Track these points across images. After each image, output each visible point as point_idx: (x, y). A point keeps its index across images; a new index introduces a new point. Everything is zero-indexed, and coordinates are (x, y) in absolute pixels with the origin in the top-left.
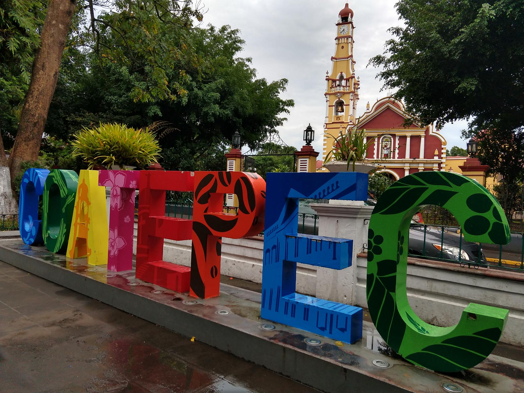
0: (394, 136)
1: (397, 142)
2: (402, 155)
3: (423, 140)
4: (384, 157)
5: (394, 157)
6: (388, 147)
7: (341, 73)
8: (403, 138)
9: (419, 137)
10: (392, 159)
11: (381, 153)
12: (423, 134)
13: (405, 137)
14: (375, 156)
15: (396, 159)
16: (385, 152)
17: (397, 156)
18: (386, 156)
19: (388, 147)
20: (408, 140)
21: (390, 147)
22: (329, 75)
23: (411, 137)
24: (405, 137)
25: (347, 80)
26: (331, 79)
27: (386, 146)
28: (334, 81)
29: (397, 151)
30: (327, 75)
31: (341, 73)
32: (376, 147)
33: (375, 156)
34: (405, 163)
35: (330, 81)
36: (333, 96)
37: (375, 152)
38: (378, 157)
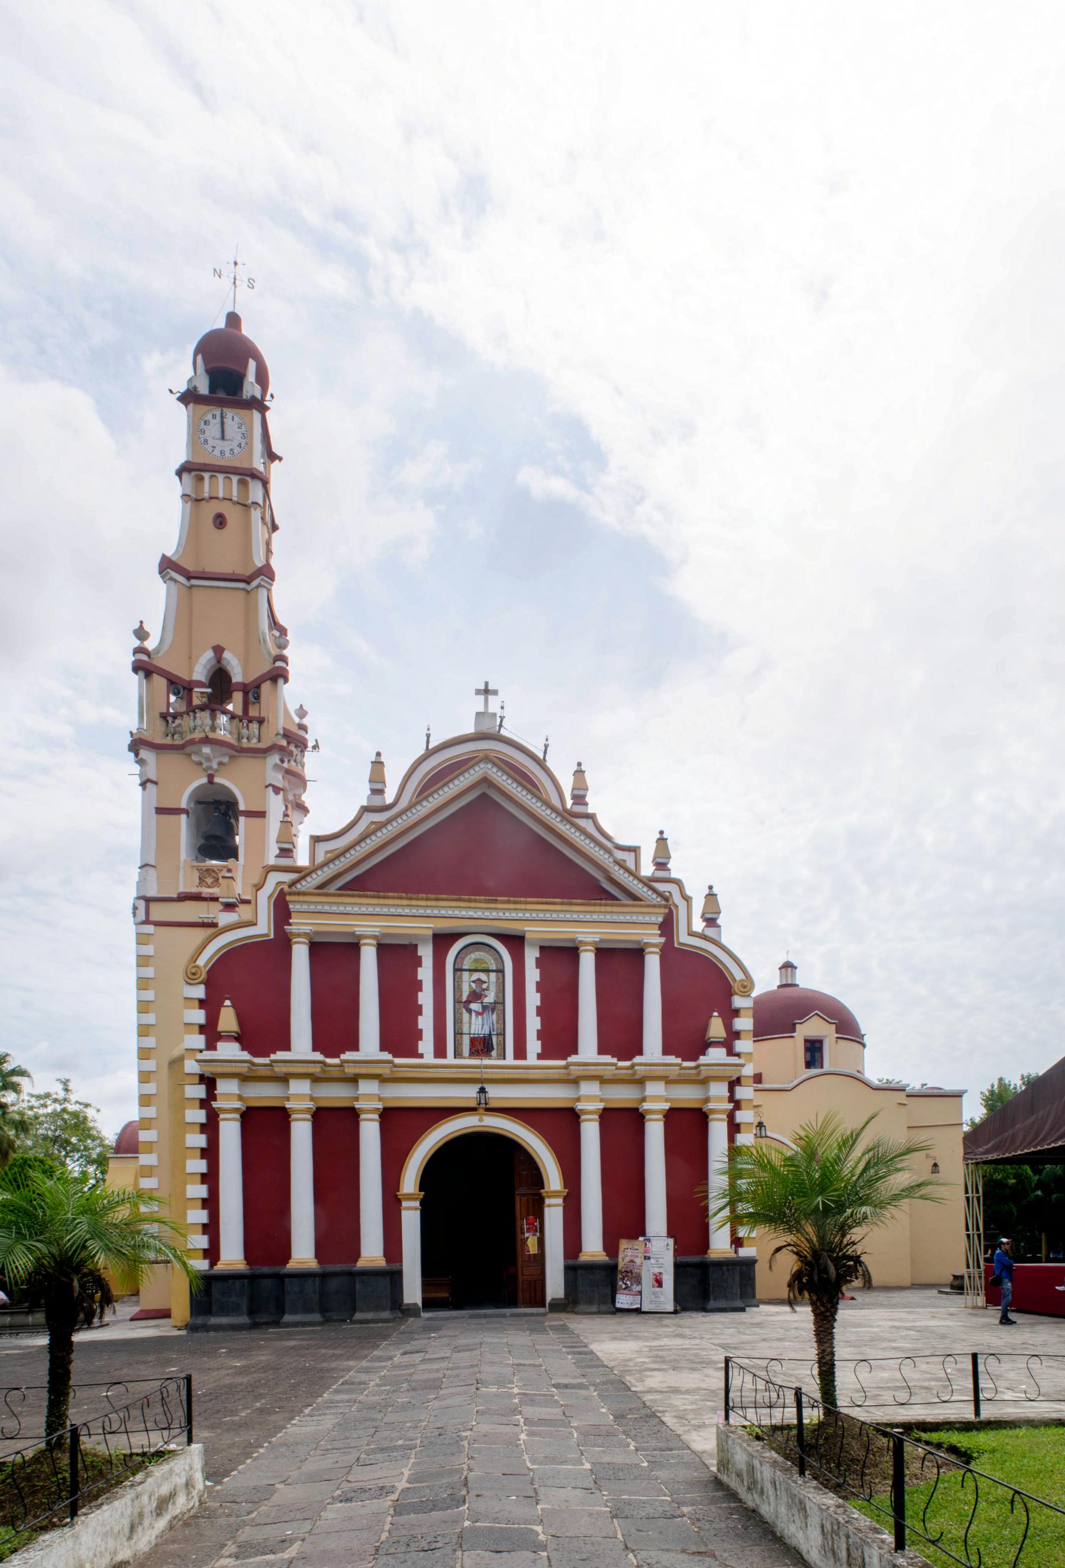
0: (515, 942)
1: (532, 975)
3: (653, 965)
5: (520, 1052)
6: (490, 998)
8: (561, 958)
9: (636, 955)
11: (458, 1034)
12: (653, 938)
13: (570, 953)
15: (532, 1059)
16: (477, 1025)
17: (534, 1046)
18: (482, 1046)
19: (490, 998)
20: (587, 962)
21: (498, 1006)
22: (151, 644)
23: (604, 954)
24: (570, 953)
27: (475, 996)
30: (137, 643)
32: (426, 998)
33: (426, 1045)
34: (575, 1082)
37: (426, 1022)
38: (440, 1051)
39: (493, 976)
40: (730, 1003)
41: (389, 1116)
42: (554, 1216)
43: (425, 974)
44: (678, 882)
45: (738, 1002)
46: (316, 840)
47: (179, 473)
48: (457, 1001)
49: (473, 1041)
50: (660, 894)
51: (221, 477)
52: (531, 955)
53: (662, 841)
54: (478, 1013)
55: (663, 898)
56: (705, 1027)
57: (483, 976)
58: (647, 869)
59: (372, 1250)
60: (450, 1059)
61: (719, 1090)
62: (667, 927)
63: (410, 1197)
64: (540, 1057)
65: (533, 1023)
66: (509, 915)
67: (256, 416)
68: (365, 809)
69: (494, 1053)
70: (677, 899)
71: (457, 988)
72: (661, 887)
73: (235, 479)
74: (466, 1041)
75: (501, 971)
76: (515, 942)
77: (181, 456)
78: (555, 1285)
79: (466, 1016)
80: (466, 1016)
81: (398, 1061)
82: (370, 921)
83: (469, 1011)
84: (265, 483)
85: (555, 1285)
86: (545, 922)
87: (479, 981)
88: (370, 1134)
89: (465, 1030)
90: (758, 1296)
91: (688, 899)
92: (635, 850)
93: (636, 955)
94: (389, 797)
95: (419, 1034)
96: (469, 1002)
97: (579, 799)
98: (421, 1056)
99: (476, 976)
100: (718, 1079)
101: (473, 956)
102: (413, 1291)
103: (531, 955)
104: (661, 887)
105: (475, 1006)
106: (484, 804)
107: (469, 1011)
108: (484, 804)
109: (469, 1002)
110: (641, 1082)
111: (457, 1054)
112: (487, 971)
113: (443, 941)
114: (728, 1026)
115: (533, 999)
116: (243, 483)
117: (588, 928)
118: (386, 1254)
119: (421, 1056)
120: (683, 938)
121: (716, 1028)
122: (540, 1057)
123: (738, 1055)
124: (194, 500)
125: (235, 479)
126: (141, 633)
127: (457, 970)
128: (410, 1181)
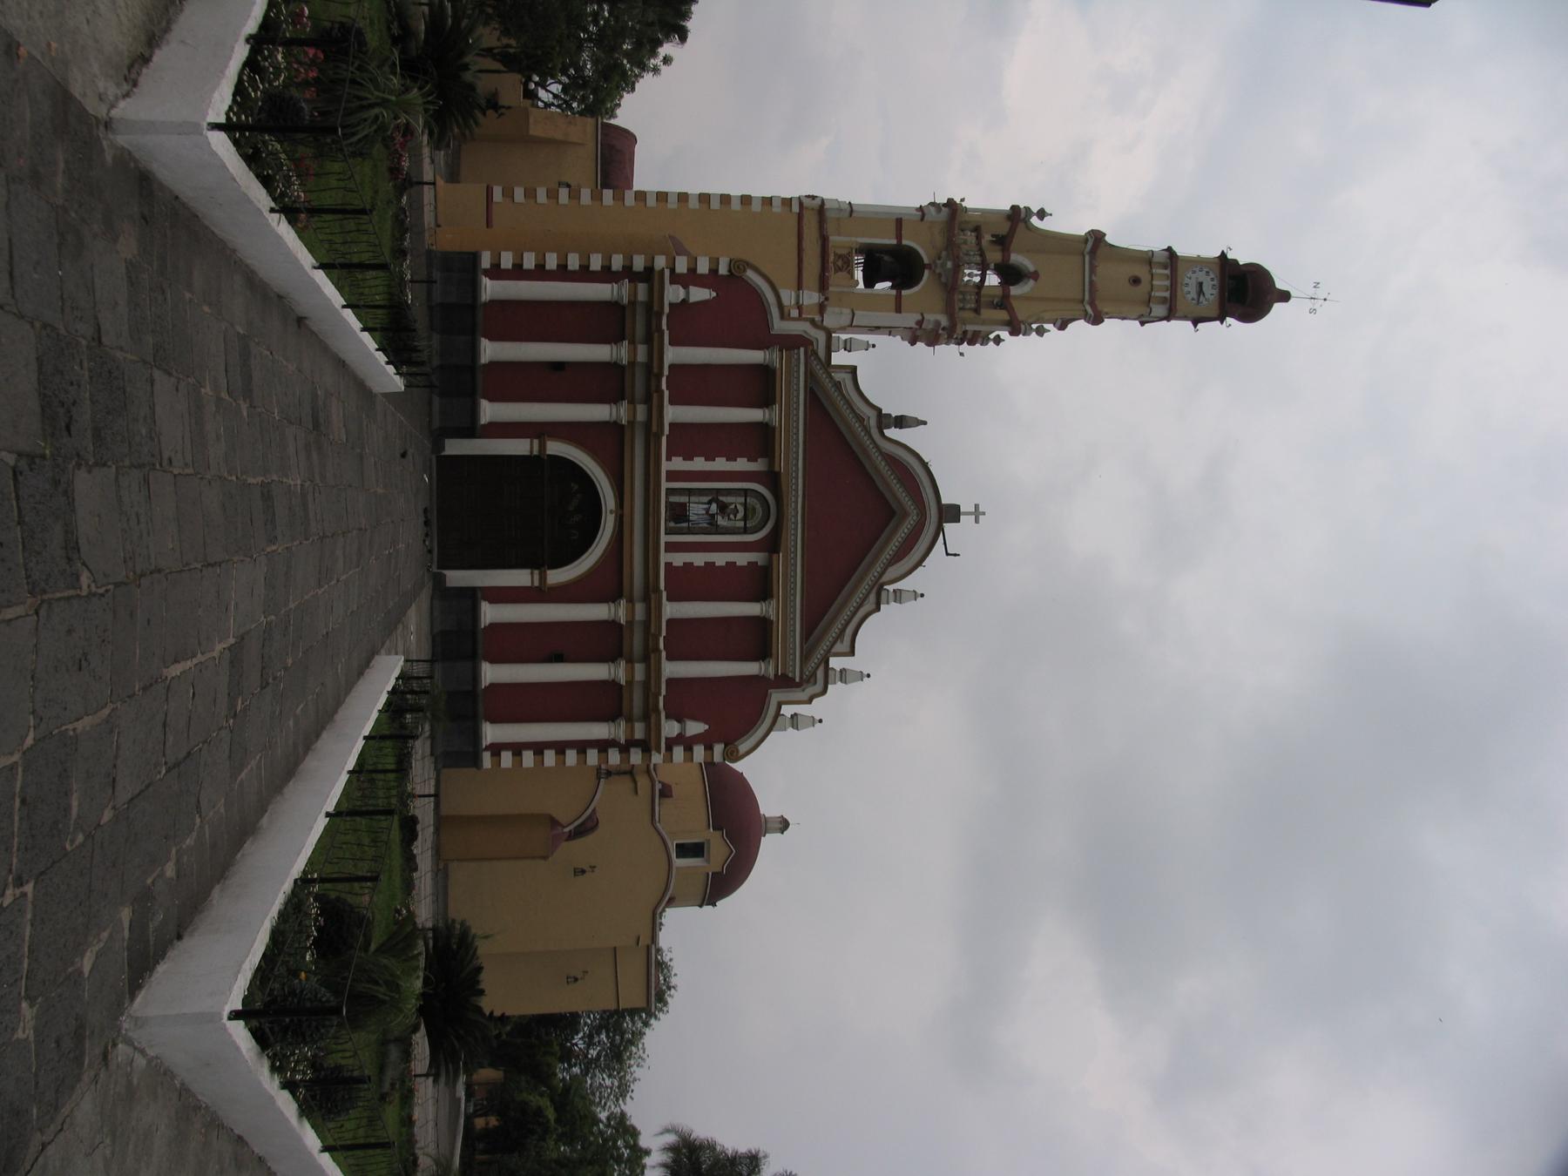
1: (741, 559)
2: (688, 584)
4: (669, 505)
5: (671, 547)
6: (721, 521)
7: (1035, 276)
8: (759, 584)
10: (664, 539)
11: (690, 492)
14: (678, 464)
16: (697, 509)
17: (679, 559)
18: (679, 514)
19: (721, 521)
21: (714, 528)
24: (763, 592)
25: (1003, 302)
26: (1013, 230)
27: (723, 508)
28: (1002, 242)
29: (699, 559)
31: (1035, 276)
32: (720, 464)
33: (678, 464)
34: (646, 599)
35: (1004, 229)
36: (939, 240)
37: (699, 464)
38: (672, 476)
39: (742, 524)
40: (719, 742)
41: (614, 430)
42: (520, 578)
43: (741, 465)
44: (824, 691)
45: (718, 749)
46: (853, 370)
47: (1169, 249)
48: (718, 491)
49: (683, 506)
50: (814, 674)
51: (1167, 283)
52: (757, 557)
53: (862, 676)
54: (707, 510)
55: (812, 677)
56: (695, 718)
57: (740, 516)
58: (835, 663)
59: (489, 411)
60: (665, 485)
61: (639, 733)
62: (785, 682)
63: (542, 447)
64: (669, 565)
65: (699, 559)
66: (795, 536)
67: (1215, 313)
68: (879, 410)
69: (672, 524)
70: (810, 690)
71: (729, 492)
72: (820, 674)
73: (1167, 294)
74: (683, 499)
75: (745, 531)
76: (772, 544)
77: (1180, 251)
78: (458, 578)
79: (706, 499)
80: (706, 499)
81: (664, 439)
82: (788, 417)
83: (710, 503)
84: (1168, 318)
85: (458, 578)
86: (792, 570)
87: (736, 511)
88: (598, 412)
89: (693, 499)
90: (445, 771)
91: (810, 701)
92: (852, 653)
93: (762, 652)
94: (892, 433)
95: (688, 457)
96: (717, 501)
97: (898, 596)
98: (669, 459)
99: (741, 508)
100: (648, 730)
101: (758, 506)
102: (456, 447)
103: (757, 557)
104: (820, 674)
105: (714, 507)
106: (892, 514)
107: (710, 503)
108: (888, 514)
109: (717, 501)
110: (646, 659)
111: (670, 492)
112: (745, 519)
113: (772, 479)
114: (697, 739)
115: (720, 559)
116: (1163, 301)
117: (784, 611)
118: (491, 424)
119: (669, 459)
120: (776, 696)
121: (695, 728)
122: (669, 565)
123: (669, 749)
124: (1147, 259)
125: (1167, 294)
126: (1042, 214)
127: (746, 492)
128: (555, 448)
